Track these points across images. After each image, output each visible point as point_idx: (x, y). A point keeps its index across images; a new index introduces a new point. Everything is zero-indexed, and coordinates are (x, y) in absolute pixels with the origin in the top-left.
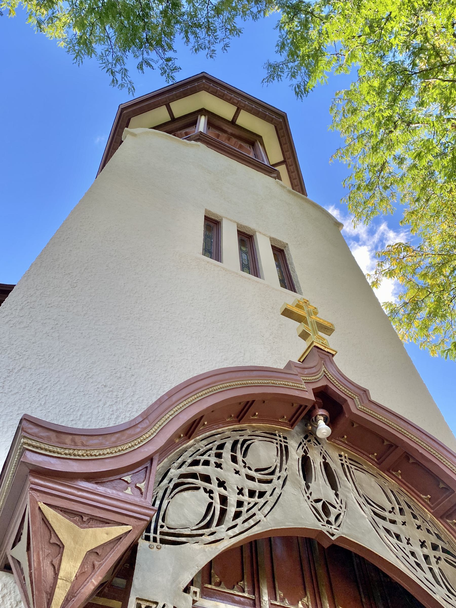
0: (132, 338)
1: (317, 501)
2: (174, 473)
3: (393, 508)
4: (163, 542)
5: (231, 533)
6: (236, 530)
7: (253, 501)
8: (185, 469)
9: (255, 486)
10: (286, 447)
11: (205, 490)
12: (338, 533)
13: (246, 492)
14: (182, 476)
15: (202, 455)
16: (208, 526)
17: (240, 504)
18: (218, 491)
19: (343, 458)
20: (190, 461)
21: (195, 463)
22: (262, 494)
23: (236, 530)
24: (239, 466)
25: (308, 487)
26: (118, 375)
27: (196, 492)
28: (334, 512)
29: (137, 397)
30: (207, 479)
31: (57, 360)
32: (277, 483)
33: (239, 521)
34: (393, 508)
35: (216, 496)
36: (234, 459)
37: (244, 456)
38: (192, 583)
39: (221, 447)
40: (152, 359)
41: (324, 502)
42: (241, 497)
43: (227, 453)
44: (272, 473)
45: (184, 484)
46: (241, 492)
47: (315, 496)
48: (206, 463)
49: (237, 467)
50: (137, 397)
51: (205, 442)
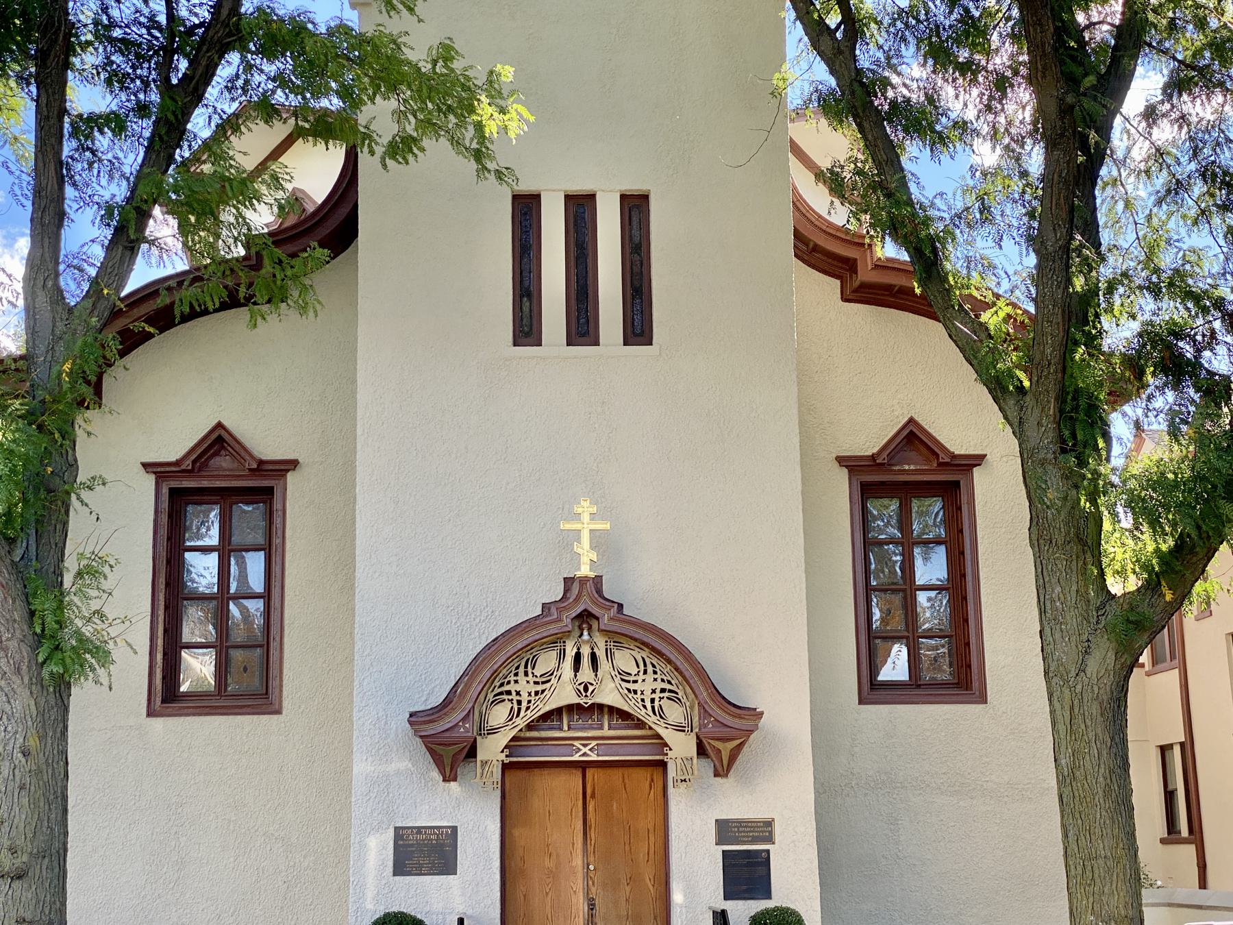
0: (458, 543)
1: (580, 684)
2: (490, 697)
3: (639, 672)
4: (488, 734)
5: (525, 719)
6: (528, 717)
7: (537, 698)
8: (497, 691)
9: (539, 688)
10: (564, 650)
11: (508, 700)
12: (590, 702)
13: (533, 694)
14: (495, 696)
15: (505, 678)
16: (511, 720)
17: (529, 702)
18: (515, 698)
19: (608, 643)
20: (498, 684)
21: (502, 685)
22: (543, 691)
23: (528, 717)
24: (530, 678)
25: (576, 676)
26: (454, 592)
27: (503, 703)
28: (591, 688)
29: (472, 606)
30: (509, 693)
31: (409, 597)
32: (554, 681)
33: (529, 712)
34: (639, 672)
35: (515, 702)
36: (526, 674)
37: (533, 669)
38: (506, 747)
39: (518, 668)
40: (477, 561)
41: (586, 685)
42: (530, 698)
43: (522, 670)
44: (552, 674)
45: (496, 700)
46: (530, 694)
47: (579, 682)
48: (509, 682)
49: (528, 679)
50: (472, 606)
51: (505, 670)
